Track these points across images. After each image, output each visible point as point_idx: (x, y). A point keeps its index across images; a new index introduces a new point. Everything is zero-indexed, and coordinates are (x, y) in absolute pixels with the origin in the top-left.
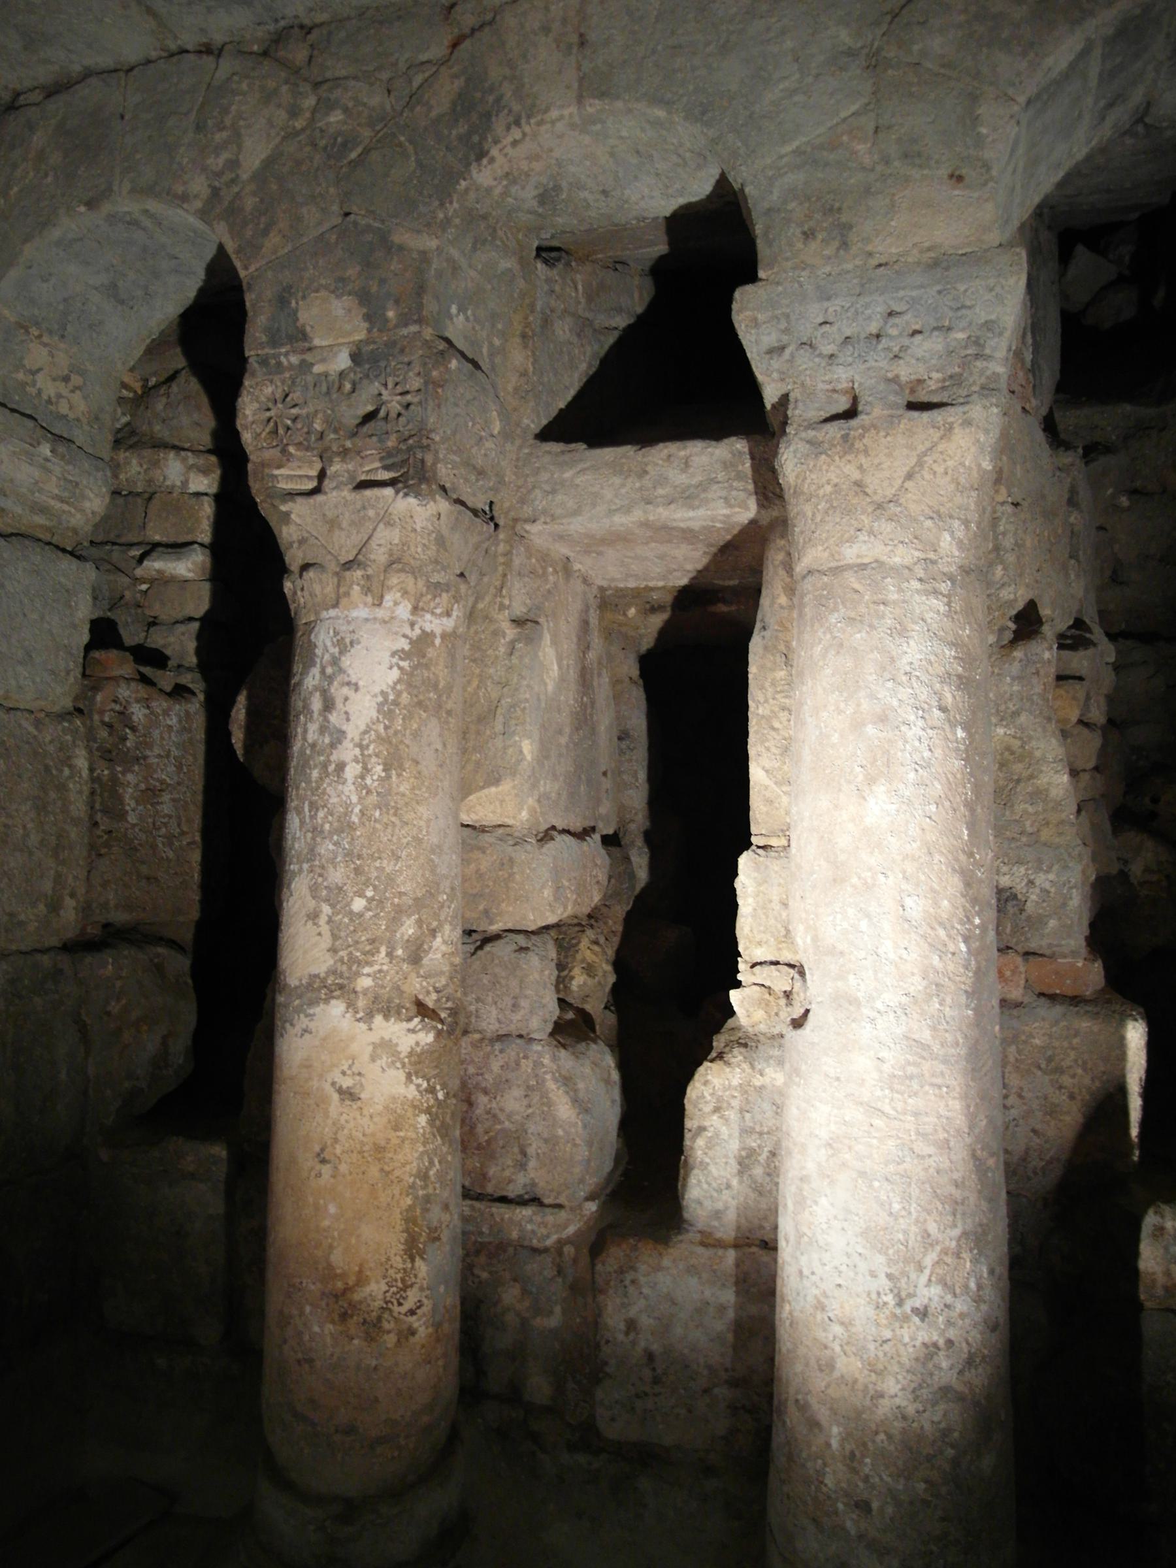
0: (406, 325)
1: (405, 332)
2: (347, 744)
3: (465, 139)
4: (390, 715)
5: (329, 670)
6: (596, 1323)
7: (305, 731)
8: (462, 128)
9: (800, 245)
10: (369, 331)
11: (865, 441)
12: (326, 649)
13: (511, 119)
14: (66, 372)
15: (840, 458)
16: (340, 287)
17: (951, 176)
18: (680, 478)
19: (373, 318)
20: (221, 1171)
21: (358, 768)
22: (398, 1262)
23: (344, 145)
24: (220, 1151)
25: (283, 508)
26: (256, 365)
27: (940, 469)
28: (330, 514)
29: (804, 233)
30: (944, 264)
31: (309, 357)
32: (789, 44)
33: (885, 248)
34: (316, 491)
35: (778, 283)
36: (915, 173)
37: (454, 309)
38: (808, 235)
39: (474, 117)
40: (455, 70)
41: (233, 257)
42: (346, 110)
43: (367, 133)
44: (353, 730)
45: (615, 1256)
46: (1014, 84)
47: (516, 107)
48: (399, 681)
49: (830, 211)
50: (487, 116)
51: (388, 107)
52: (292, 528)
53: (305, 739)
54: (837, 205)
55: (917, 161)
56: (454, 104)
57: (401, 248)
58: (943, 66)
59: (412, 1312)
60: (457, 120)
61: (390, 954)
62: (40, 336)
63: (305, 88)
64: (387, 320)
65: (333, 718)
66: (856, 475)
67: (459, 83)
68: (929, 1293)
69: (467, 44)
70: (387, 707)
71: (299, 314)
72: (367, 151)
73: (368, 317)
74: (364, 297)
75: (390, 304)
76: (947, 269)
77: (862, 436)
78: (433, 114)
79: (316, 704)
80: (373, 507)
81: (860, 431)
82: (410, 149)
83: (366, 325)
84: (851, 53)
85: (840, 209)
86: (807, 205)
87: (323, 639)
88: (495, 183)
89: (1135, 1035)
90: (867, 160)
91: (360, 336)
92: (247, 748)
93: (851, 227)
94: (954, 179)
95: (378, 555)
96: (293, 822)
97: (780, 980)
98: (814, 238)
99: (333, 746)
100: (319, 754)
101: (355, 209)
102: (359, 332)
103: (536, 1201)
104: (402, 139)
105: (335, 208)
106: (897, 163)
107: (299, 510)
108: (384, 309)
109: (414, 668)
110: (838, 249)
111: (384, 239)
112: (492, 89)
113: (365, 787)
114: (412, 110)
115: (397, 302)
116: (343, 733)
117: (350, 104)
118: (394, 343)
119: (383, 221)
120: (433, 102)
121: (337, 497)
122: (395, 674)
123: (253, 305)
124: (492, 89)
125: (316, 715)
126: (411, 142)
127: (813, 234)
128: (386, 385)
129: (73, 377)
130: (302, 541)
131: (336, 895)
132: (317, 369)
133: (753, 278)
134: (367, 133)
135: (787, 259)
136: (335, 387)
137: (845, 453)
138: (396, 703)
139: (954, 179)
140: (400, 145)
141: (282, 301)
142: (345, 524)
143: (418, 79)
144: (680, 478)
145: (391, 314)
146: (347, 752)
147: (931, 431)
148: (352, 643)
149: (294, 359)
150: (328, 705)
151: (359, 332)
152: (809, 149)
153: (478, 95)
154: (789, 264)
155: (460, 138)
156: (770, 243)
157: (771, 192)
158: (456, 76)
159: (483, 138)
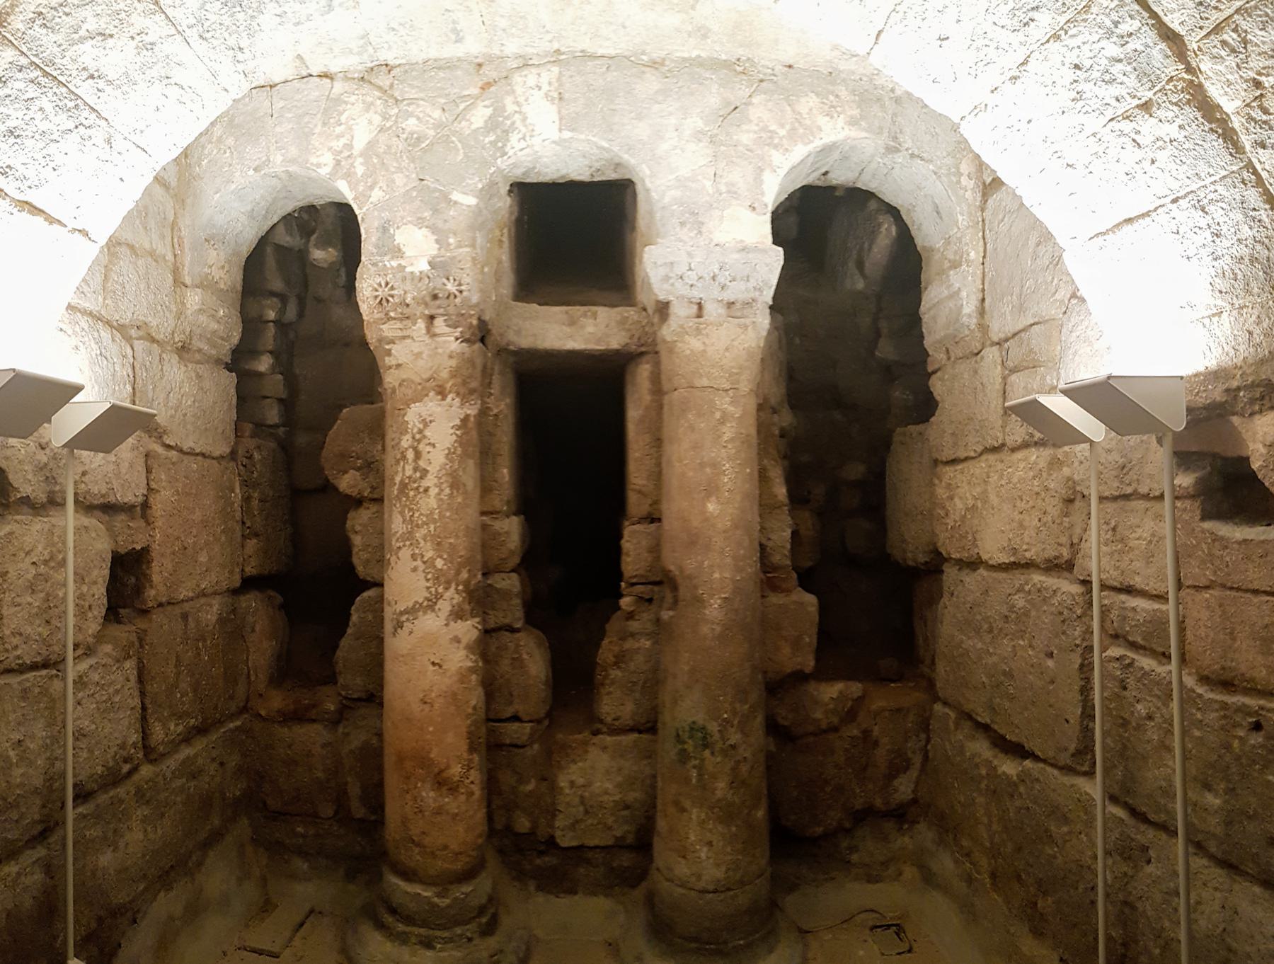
0: (461, 247)
1: (461, 250)
2: (429, 476)
4: (451, 461)
5: (418, 436)
7: (404, 468)
9: (678, 229)
10: (439, 249)
12: (414, 425)
13: (520, 136)
16: (420, 222)
21: (437, 490)
22: (465, 755)
23: (418, 139)
25: (387, 347)
28: (416, 351)
31: (403, 262)
36: (734, 202)
38: (682, 224)
39: (499, 132)
40: (486, 103)
43: (432, 133)
44: (433, 469)
48: (455, 441)
49: (693, 213)
51: (444, 119)
52: (391, 358)
53: (404, 475)
57: (456, 203)
59: (472, 783)
60: (489, 132)
61: (456, 589)
63: (391, 101)
64: (449, 244)
65: (422, 463)
66: (702, 348)
67: (489, 111)
69: (493, 89)
72: (432, 144)
73: (437, 241)
74: (434, 229)
75: (451, 235)
78: (473, 127)
79: (410, 455)
82: (459, 145)
83: (437, 246)
84: (701, 132)
90: (711, 192)
91: (435, 252)
93: (703, 224)
99: (421, 478)
100: (415, 482)
101: (427, 177)
102: (432, 249)
104: (454, 139)
105: (414, 176)
108: (448, 238)
109: (463, 434)
111: (445, 197)
112: (507, 118)
113: (441, 499)
114: (460, 123)
115: (455, 234)
116: (427, 471)
117: (421, 115)
118: (454, 257)
119: (444, 186)
120: (473, 119)
122: (454, 437)
124: (507, 118)
125: (410, 461)
126: (460, 141)
128: (448, 279)
130: (399, 366)
132: (409, 269)
134: (432, 133)
138: (454, 453)
140: (453, 142)
142: (424, 356)
143: (462, 106)
145: (451, 240)
146: (430, 481)
148: (431, 422)
149: (394, 263)
150: (418, 455)
151: (432, 249)
153: (501, 119)
158: (485, 106)
159: (505, 145)
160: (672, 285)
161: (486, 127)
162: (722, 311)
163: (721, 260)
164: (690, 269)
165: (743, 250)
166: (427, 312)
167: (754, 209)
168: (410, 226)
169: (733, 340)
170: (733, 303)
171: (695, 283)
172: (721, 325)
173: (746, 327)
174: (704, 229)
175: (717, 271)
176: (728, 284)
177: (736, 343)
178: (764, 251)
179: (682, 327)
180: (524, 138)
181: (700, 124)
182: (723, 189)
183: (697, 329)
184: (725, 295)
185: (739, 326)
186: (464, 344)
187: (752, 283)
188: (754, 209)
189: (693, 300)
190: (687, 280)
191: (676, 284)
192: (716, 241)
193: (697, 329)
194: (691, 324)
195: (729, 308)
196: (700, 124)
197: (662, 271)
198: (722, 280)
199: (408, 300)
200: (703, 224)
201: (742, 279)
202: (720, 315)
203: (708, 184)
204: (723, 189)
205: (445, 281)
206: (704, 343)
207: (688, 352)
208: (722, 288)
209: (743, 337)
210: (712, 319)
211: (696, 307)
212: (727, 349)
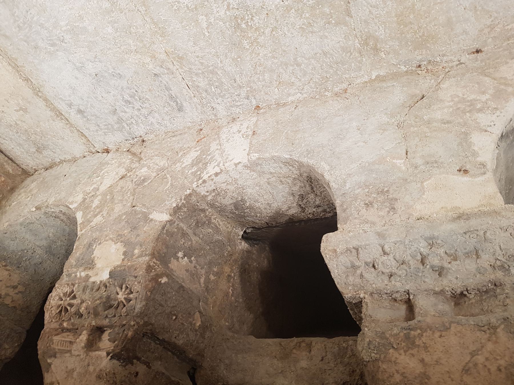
3: (194, 174)
8: (195, 169)
11: (424, 339)
14: (16, 284)
15: (405, 352)
17: (460, 171)
23: (143, 180)
26: (65, 276)
27: (493, 369)
29: (366, 204)
30: (465, 217)
32: (355, 124)
35: (349, 232)
37: (180, 254)
38: (369, 205)
41: (78, 226)
42: (149, 167)
46: (491, 126)
47: (219, 159)
50: (206, 164)
54: (386, 189)
55: (435, 165)
56: (193, 161)
58: (445, 123)
60: (193, 166)
62: (5, 266)
71: (95, 252)
76: (468, 219)
77: (421, 336)
80: (93, 364)
81: (419, 331)
85: (388, 191)
86: (367, 190)
88: (208, 194)
94: (462, 172)
98: (373, 207)
106: (423, 167)
108: (134, 249)
110: (389, 212)
123: (77, 247)
127: (371, 204)
129: (19, 286)
132: (92, 280)
133: (333, 228)
135: (356, 218)
137: (409, 348)
139: (462, 172)
147: (478, 334)
152: (367, 164)
154: (357, 221)
155: (192, 173)
156: (344, 211)
157: (346, 186)
160: (362, 276)
161: (192, 164)
162: (446, 307)
163: (428, 234)
164: (385, 253)
165: (459, 217)
166: (93, 323)
167: (466, 171)
168: (110, 241)
169: (473, 354)
170: (462, 294)
171: (394, 270)
172: (448, 329)
173: (493, 328)
174: (397, 205)
175: (425, 251)
176: (446, 265)
177: (480, 359)
178: (496, 213)
179: (382, 335)
180: (218, 165)
181: (385, 119)
182: (419, 161)
183: (407, 337)
184: (445, 282)
185: (480, 327)
186: (115, 361)
187: (486, 259)
188: (466, 171)
189: (397, 296)
190: (380, 267)
191: (366, 275)
192: (416, 215)
193: (407, 337)
194: (396, 331)
195: (457, 304)
196: (385, 119)
197: (345, 260)
198: (436, 262)
199: (82, 310)
200: (396, 200)
201: (467, 255)
202: (442, 314)
203: (399, 162)
204: (419, 161)
205: (118, 289)
206: (422, 361)
207: (397, 378)
208: (440, 275)
209: (490, 346)
210: (429, 320)
211: (404, 307)
212: (466, 370)
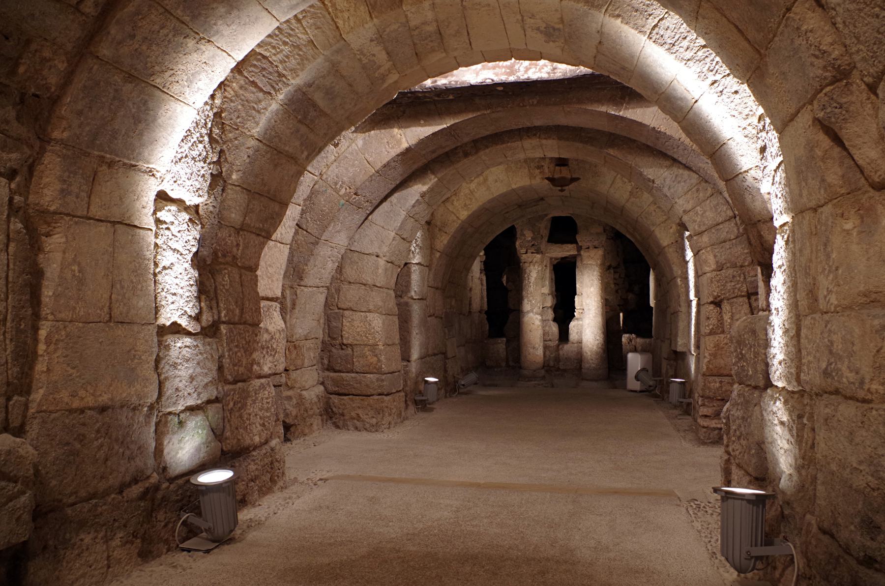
6: (559, 355)
18: (567, 249)
19: (534, 233)
20: (504, 342)
24: (505, 339)
33: (592, 232)
34: (526, 253)
45: (561, 346)
68: (598, 338)
70: (536, 279)
87: (527, 271)
89: (621, 315)
92: (507, 282)
95: (534, 261)
96: (524, 293)
97: (581, 311)
103: (550, 340)
107: (524, 255)
121: (529, 254)
131: (531, 301)
136: (529, 241)
141: (522, 230)
144: (567, 249)
146: (531, 284)
